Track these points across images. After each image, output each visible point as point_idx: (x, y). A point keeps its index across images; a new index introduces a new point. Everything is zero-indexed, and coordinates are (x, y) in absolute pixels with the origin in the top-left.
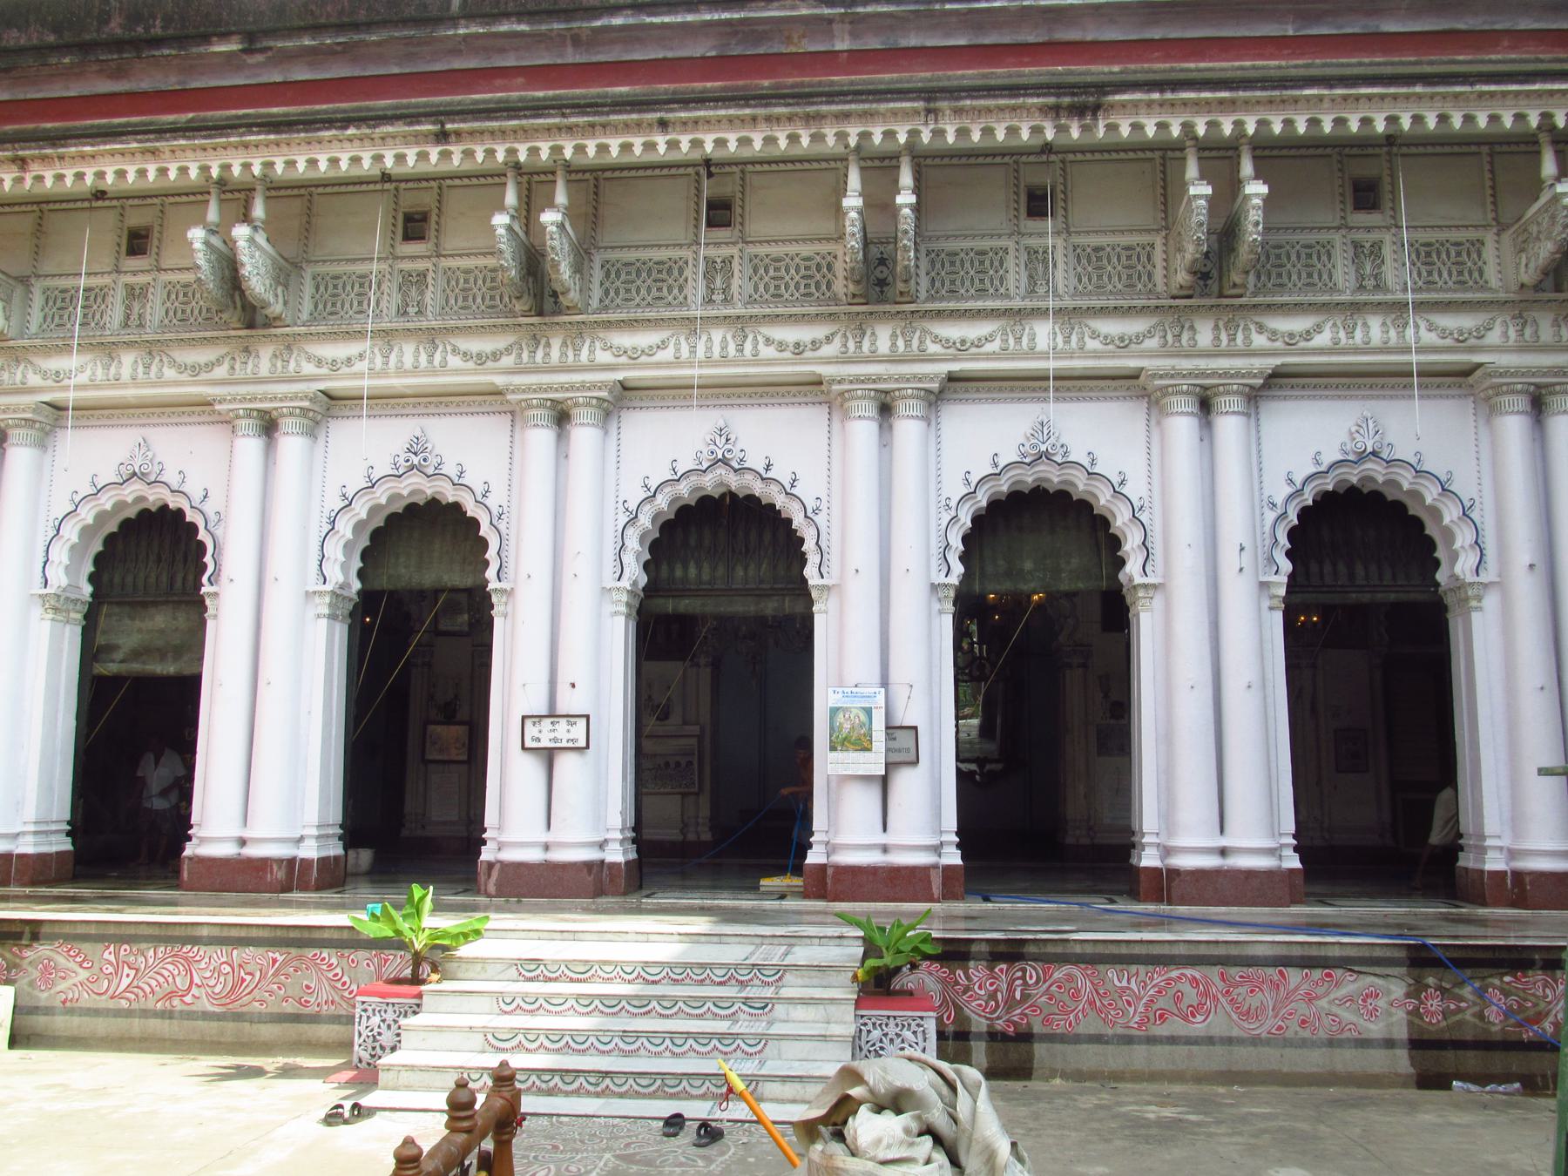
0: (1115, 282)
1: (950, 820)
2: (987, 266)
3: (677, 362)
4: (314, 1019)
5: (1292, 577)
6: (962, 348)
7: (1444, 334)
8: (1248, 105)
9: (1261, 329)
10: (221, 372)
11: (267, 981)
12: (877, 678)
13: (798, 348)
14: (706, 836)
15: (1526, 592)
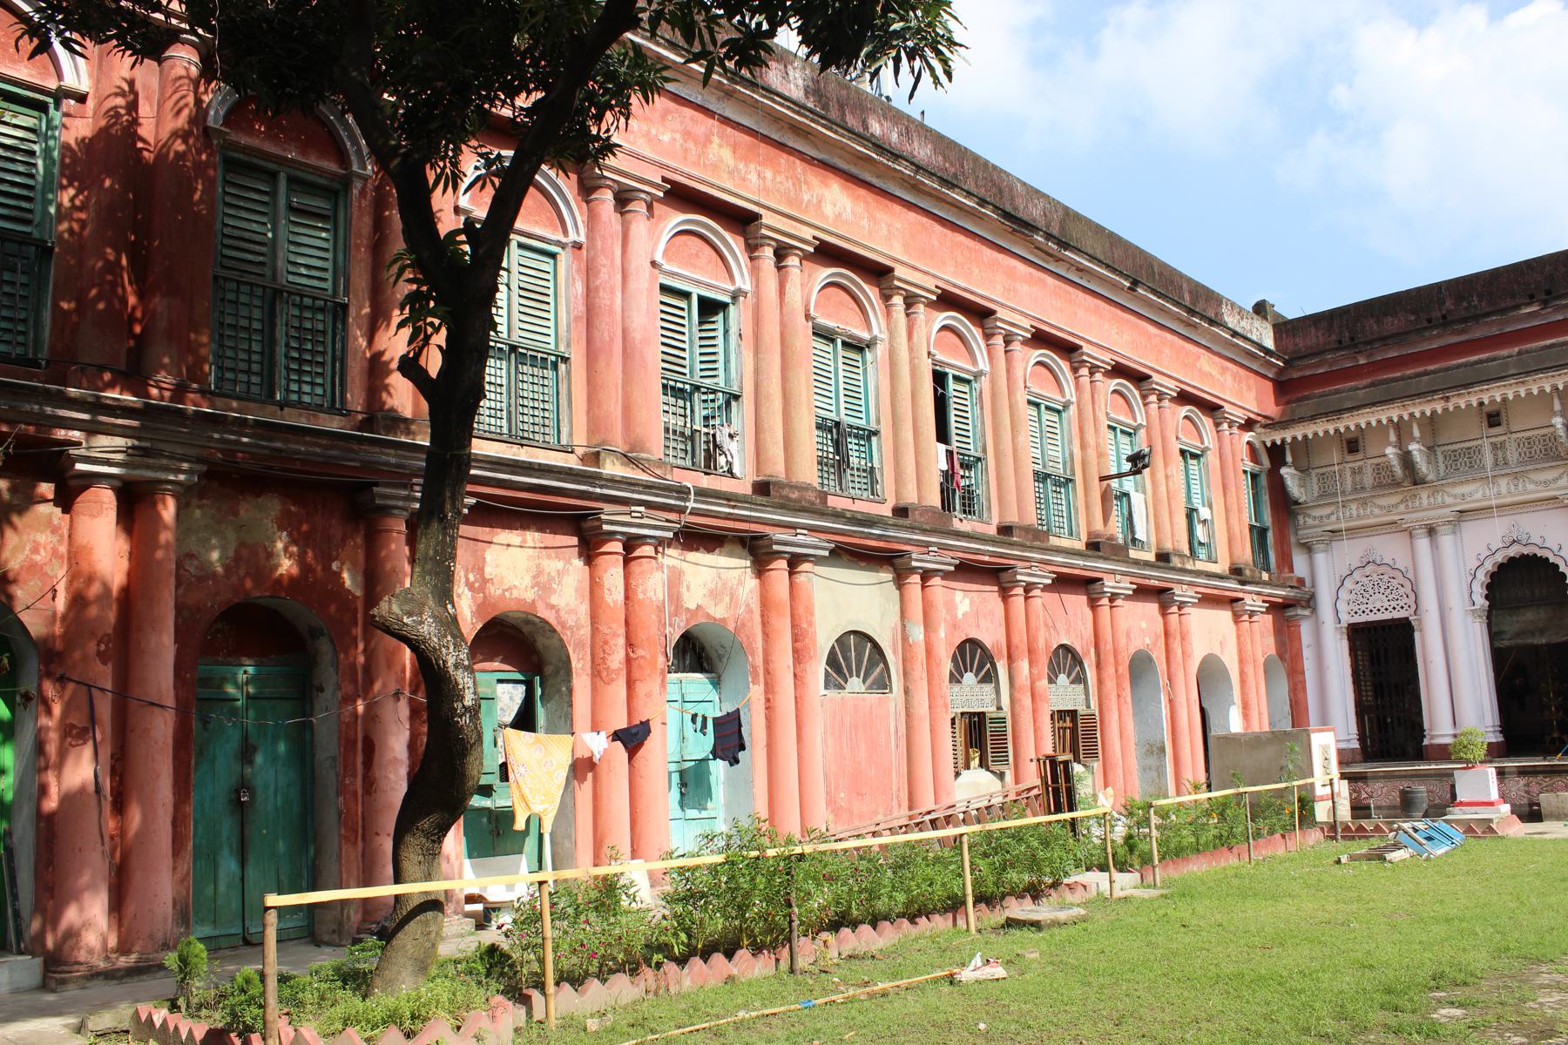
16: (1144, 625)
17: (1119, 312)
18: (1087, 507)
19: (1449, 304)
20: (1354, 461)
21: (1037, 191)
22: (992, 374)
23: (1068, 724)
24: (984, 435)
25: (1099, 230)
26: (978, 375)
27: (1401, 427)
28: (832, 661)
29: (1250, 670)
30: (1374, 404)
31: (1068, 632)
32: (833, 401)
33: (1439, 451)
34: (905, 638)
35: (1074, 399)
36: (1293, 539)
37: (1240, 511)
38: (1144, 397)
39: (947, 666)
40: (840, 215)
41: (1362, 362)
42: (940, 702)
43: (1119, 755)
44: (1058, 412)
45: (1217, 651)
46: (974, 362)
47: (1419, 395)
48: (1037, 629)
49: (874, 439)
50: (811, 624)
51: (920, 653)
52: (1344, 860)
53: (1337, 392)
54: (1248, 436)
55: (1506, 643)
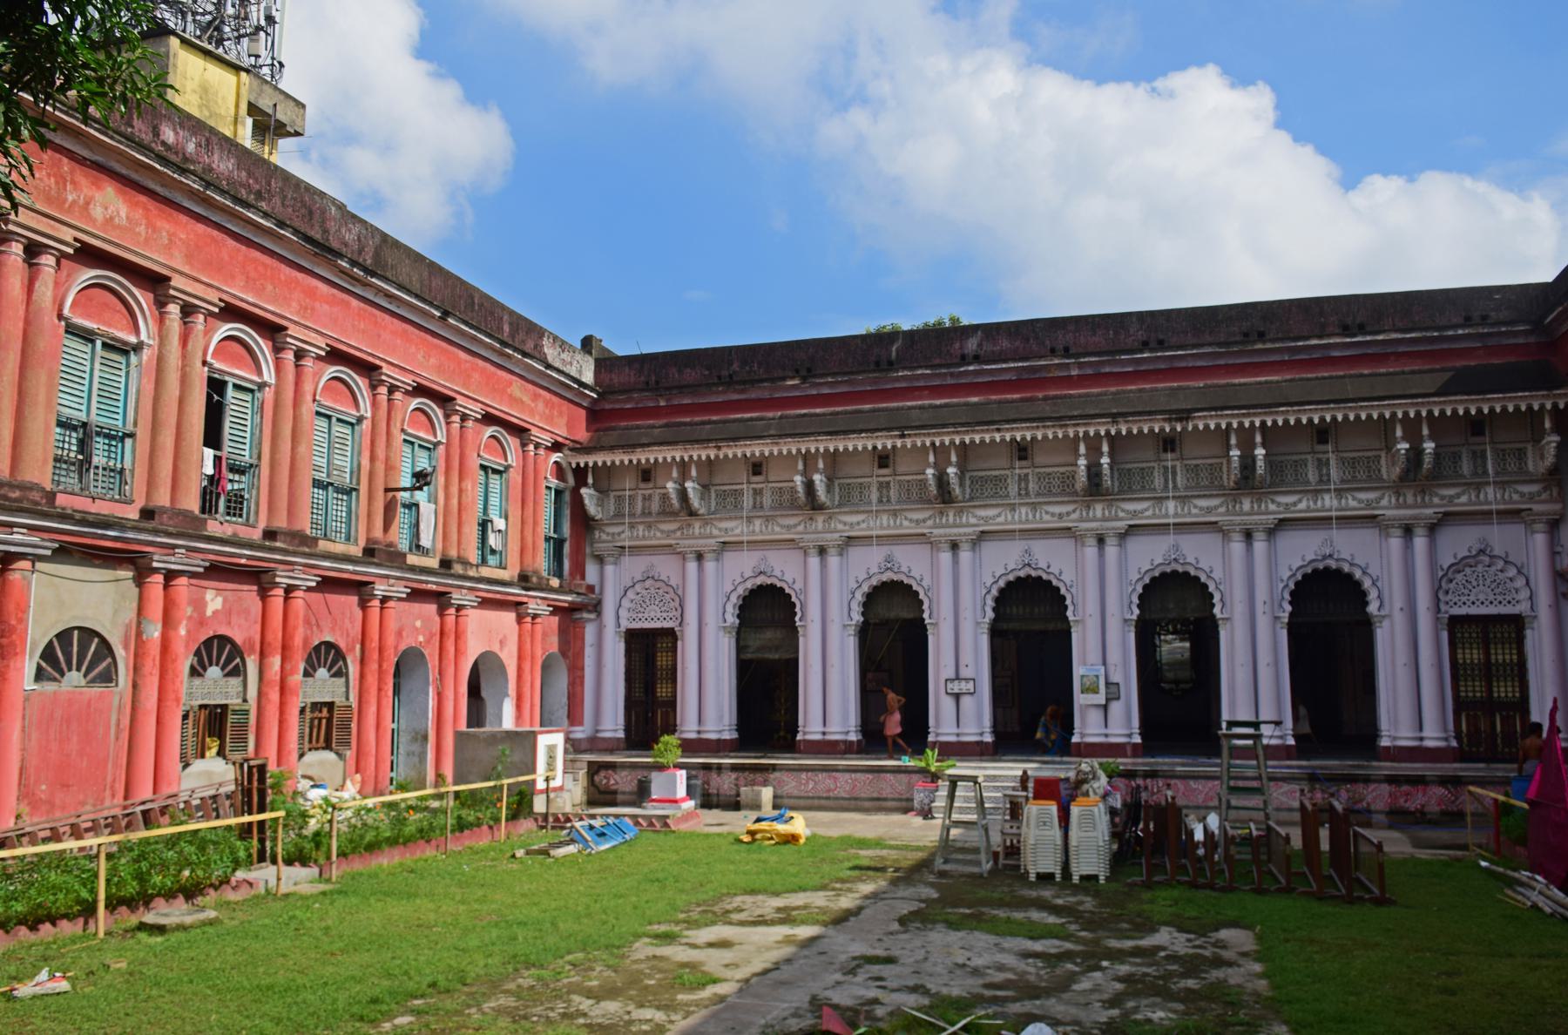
0: (1206, 481)
1: (1136, 722)
2: (1145, 474)
3: (1006, 523)
4: (885, 799)
5: (1291, 615)
6: (1135, 514)
7: (1360, 501)
8: (1255, 415)
9: (1273, 501)
10: (800, 528)
11: (865, 785)
12: (1100, 661)
13: (1061, 516)
14: (1017, 729)
15: (1399, 619)
16: (418, 624)
17: (429, 338)
18: (369, 515)
19: (735, 366)
20: (646, 489)
21: (354, 216)
22: (278, 386)
23: (325, 713)
24: (260, 443)
25: (418, 258)
26: (262, 386)
27: (684, 466)
28: (48, 654)
29: (527, 666)
30: (661, 444)
31: (333, 630)
32: (85, 401)
33: (713, 489)
34: (139, 634)
35: (369, 415)
36: (588, 550)
37: (535, 523)
38: (447, 416)
39: (186, 662)
40: (112, 218)
41: (662, 403)
42: (171, 696)
43: (373, 743)
44: (352, 425)
45: (496, 648)
46: (259, 372)
47: (697, 441)
48: (295, 628)
49: (128, 442)
50: (20, 621)
51: (154, 651)
52: (520, 853)
53: (638, 427)
54: (556, 457)
55: (749, 656)
